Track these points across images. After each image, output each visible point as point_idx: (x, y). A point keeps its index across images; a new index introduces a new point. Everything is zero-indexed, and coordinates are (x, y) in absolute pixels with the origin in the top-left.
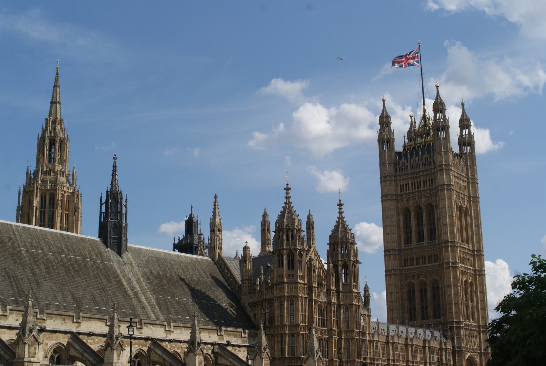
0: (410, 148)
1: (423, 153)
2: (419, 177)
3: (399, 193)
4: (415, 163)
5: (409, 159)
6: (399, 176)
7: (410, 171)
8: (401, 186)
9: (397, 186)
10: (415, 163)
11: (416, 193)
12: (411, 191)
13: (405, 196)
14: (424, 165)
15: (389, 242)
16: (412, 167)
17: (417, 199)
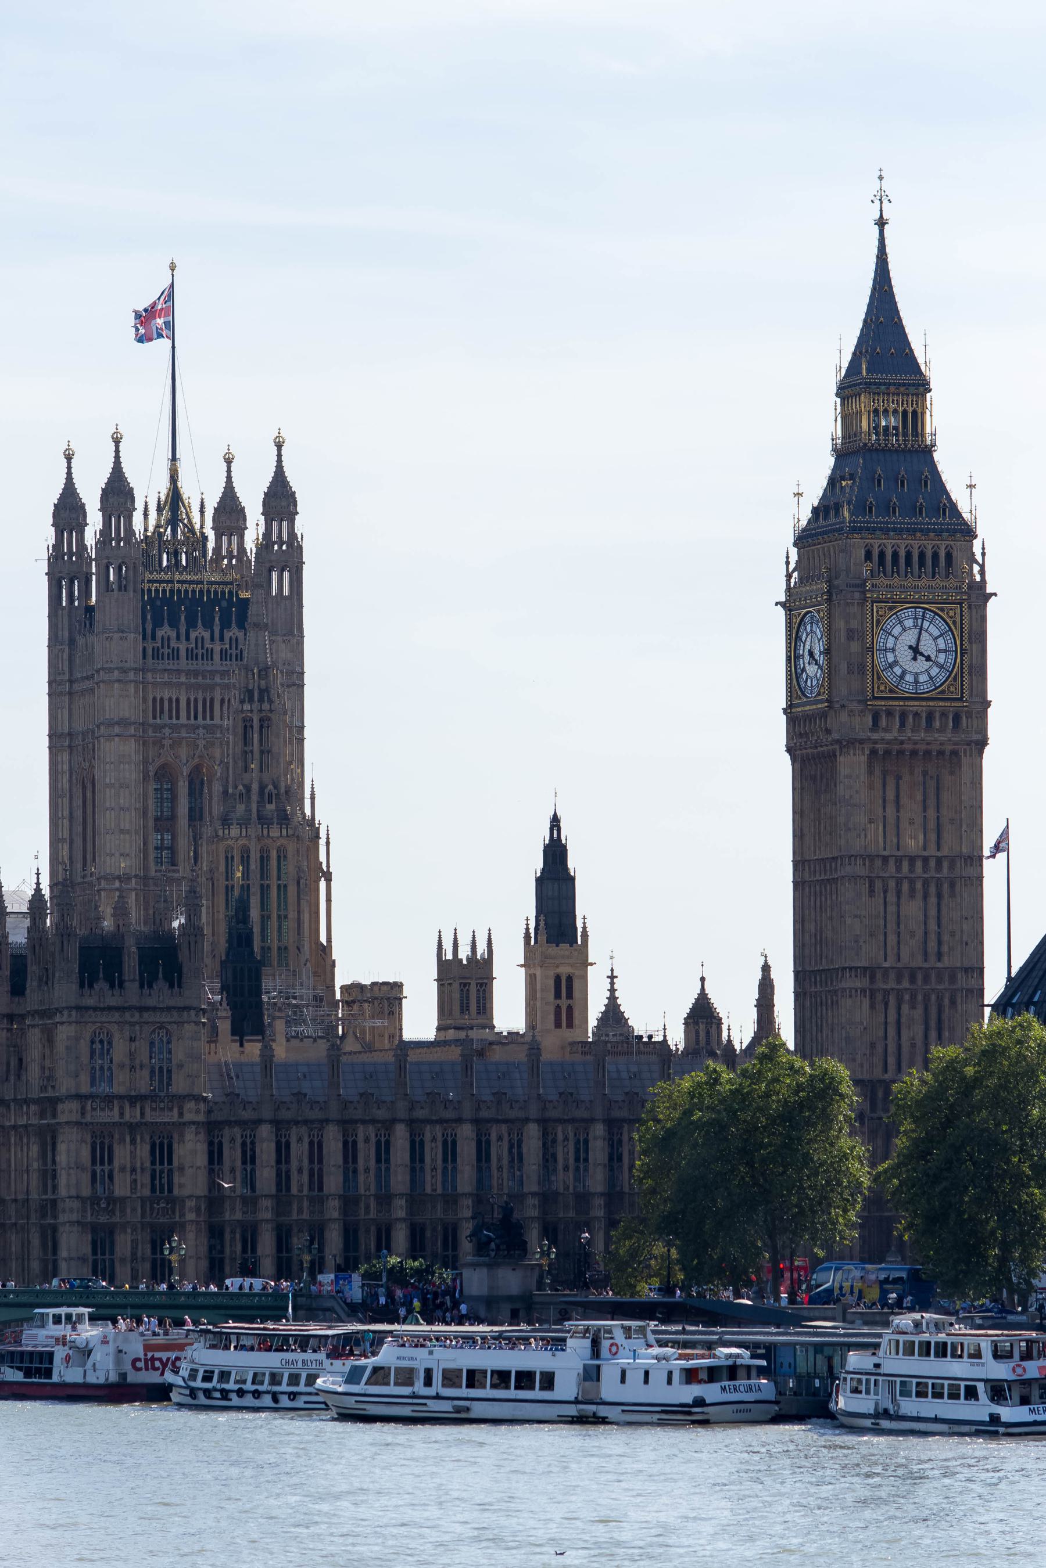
0: (164, 591)
1: (225, 625)
2: (212, 687)
3: (151, 721)
4: (200, 645)
5: (183, 631)
6: (154, 671)
7: (183, 663)
8: (154, 699)
9: (145, 700)
10: (200, 645)
11: (201, 731)
12: (183, 720)
13: (167, 731)
14: (224, 655)
15: (128, 855)
16: (191, 655)
17: (201, 746)
